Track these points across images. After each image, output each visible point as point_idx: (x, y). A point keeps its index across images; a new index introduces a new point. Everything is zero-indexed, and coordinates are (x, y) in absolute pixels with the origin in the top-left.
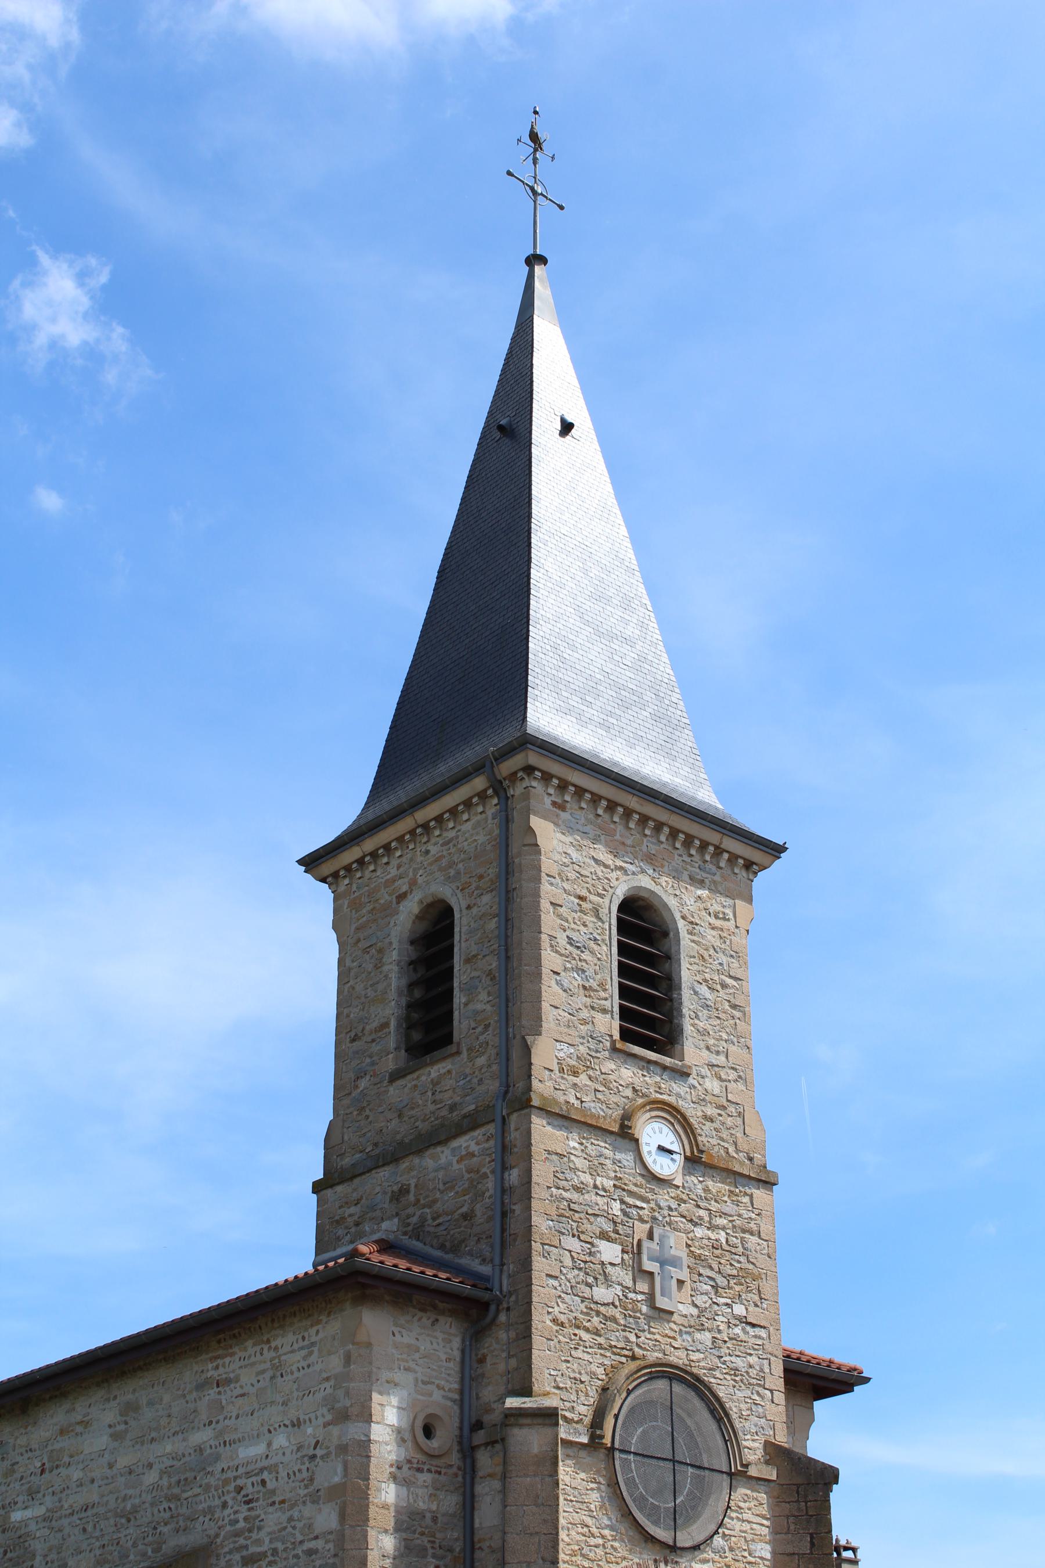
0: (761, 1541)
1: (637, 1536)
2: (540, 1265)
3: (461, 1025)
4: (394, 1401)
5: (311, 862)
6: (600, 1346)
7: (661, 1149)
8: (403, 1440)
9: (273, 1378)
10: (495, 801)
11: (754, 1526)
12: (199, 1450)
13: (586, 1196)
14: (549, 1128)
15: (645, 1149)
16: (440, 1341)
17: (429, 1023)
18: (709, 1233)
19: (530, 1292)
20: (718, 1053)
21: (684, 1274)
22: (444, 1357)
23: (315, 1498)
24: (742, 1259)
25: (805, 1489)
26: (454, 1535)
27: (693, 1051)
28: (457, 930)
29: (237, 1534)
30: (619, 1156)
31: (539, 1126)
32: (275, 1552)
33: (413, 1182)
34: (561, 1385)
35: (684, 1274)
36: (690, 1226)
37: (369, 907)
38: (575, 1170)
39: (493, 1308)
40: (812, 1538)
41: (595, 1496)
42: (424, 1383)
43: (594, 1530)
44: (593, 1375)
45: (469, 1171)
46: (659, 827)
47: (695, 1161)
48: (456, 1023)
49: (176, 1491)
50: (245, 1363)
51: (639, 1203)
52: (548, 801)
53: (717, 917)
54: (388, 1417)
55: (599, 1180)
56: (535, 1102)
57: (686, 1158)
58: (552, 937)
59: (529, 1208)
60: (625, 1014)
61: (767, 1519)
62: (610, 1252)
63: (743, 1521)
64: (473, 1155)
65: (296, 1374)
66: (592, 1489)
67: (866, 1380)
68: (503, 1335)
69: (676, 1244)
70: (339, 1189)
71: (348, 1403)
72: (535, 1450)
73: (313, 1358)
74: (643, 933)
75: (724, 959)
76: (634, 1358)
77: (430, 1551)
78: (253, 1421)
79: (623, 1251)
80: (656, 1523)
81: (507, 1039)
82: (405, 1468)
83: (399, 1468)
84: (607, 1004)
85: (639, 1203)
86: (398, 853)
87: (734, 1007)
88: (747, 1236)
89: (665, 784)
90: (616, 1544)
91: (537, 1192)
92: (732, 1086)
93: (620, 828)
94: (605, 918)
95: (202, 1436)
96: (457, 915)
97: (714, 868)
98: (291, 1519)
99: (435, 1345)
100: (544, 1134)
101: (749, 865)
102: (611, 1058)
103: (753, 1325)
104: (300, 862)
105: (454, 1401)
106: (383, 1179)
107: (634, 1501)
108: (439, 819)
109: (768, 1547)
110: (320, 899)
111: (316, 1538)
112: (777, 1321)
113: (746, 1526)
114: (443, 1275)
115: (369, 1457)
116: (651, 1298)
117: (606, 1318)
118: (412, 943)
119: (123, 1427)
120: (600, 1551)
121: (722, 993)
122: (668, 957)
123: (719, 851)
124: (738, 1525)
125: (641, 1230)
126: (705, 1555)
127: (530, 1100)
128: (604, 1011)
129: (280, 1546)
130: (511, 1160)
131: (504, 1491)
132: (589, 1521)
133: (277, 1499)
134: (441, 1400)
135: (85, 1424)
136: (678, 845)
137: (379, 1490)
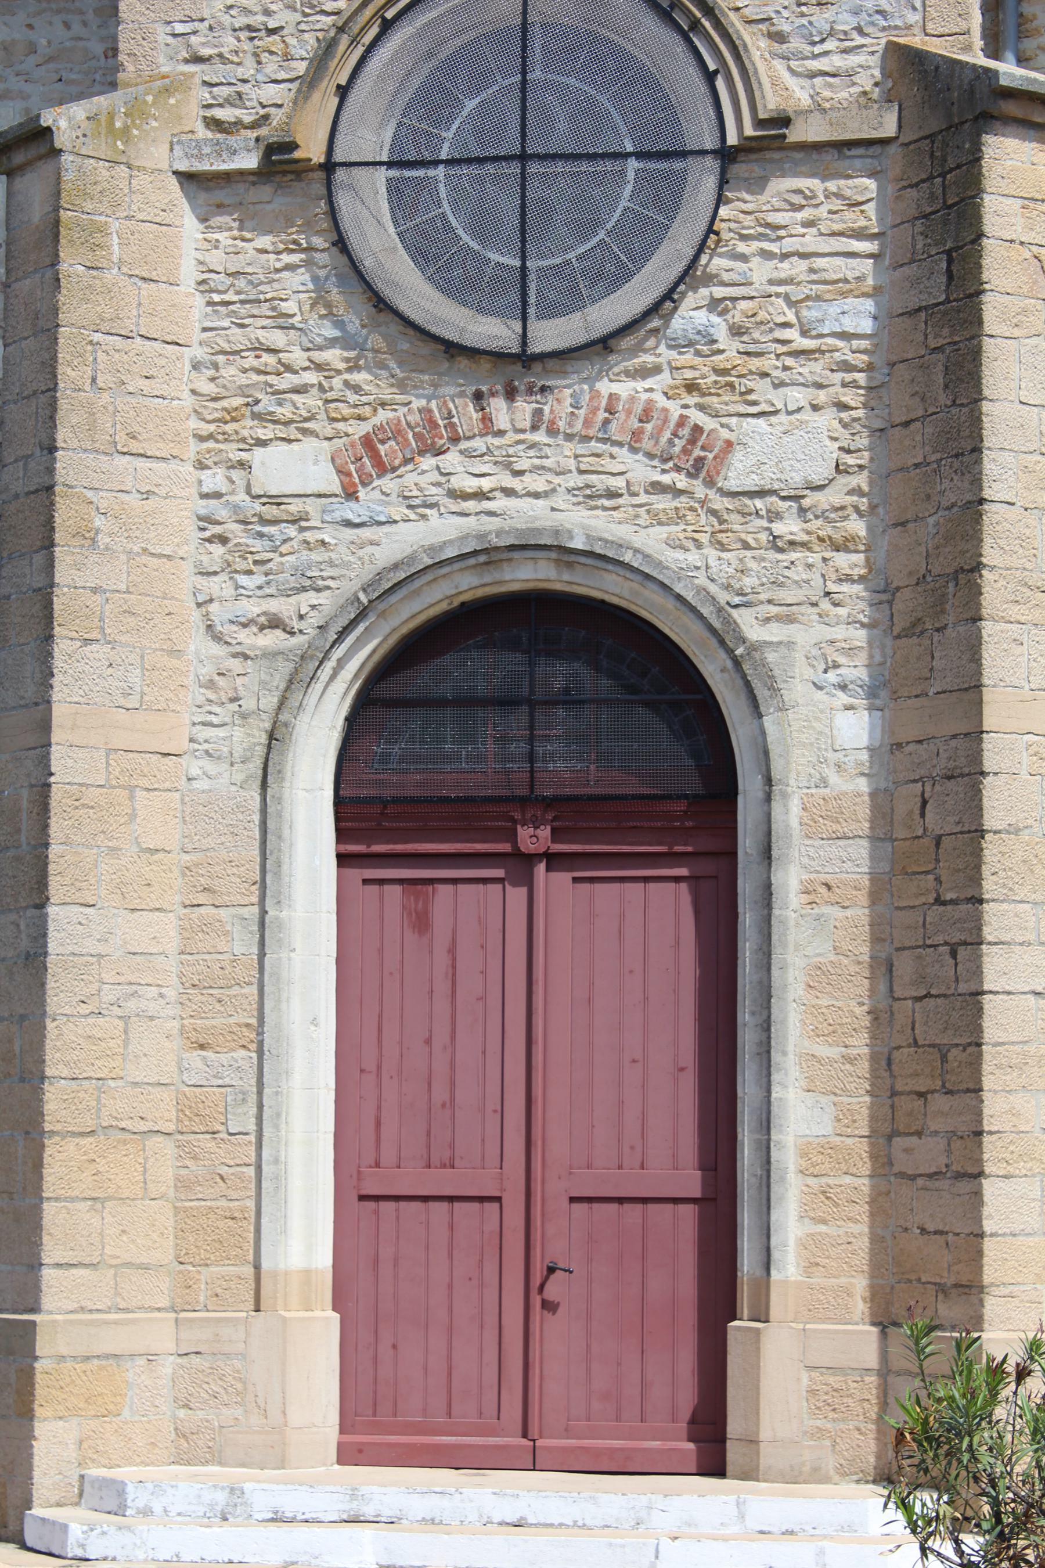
0: (844, 294)
1: (426, 349)
11: (820, 263)
16: (90, 16)
34: (206, 52)
40: (950, 261)
41: (300, 279)
43: (297, 357)
61: (873, 237)
63: (785, 256)
66: (288, 267)
90: (359, 377)
99: (77, 28)
113: (797, 268)
120: (311, 401)
124: (760, 272)
126: (648, 359)
132: (277, 338)
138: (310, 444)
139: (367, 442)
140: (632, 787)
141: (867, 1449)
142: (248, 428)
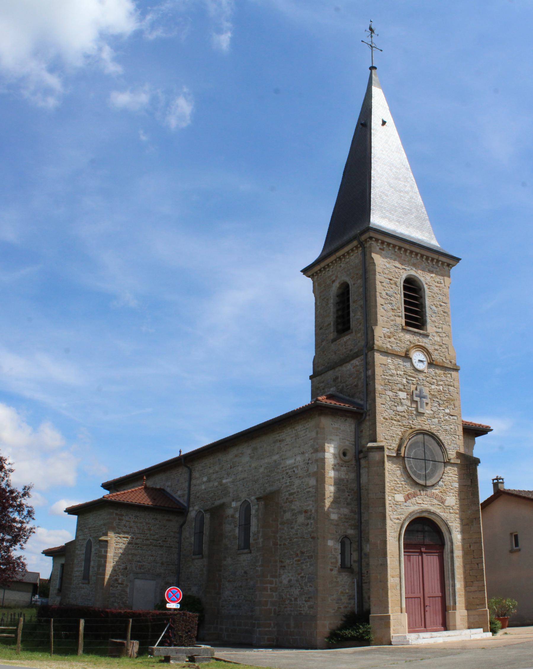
2: (378, 401)
3: (353, 324)
4: (333, 445)
5: (305, 271)
6: (400, 425)
7: (420, 361)
8: (336, 457)
9: (296, 439)
10: (361, 249)
12: (275, 461)
13: (394, 378)
14: (381, 356)
15: (414, 361)
17: (343, 324)
18: (437, 387)
19: (375, 409)
20: (439, 328)
21: (428, 401)
22: (349, 431)
23: (309, 476)
24: (448, 395)
25: (469, 466)
26: (354, 486)
27: (430, 328)
28: (350, 292)
29: (287, 487)
30: (405, 364)
31: (377, 355)
32: (298, 492)
33: (339, 375)
35: (428, 401)
36: (430, 385)
37: (323, 285)
38: (390, 369)
39: (364, 415)
41: (399, 472)
42: (343, 439)
43: (399, 482)
44: (398, 434)
45: (356, 371)
46: (417, 254)
47: (431, 364)
48: (351, 323)
49: (269, 474)
50: (287, 435)
51: (412, 379)
52: (378, 248)
53: (438, 283)
54: (330, 451)
55: (398, 372)
56: (376, 348)
57: (428, 363)
58: (380, 293)
59: (374, 383)
60: (407, 317)
62: (402, 395)
64: (357, 366)
65: (302, 438)
67: (492, 430)
68: (368, 423)
69: (426, 391)
70: (317, 378)
71: (318, 446)
72: (377, 459)
73: (307, 433)
74: (413, 290)
75: (441, 297)
76: (411, 428)
77: (346, 491)
78: (289, 452)
79: (407, 395)
80: (419, 479)
81: (367, 328)
82: (337, 466)
83: (335, 466)
84: (400, 314)
85: (412, 379)
86: (332, 267)
87: (444, 312)
88: (450, 387)
89: (419, 240)
90: (406, 486)
91: (377, 377)
92: (444, 339)
93: (403, 255)
94: (399, 286)
95: (276, 457)
96: (350, 287)
97: (437, 267)
98: (302, 482)
100: (378, 358)
101: (448, 265)
102: (402, 332)
103: (452, 416)
104: (302, 271)
105: (353, 444)
106: (330, 375)
107: (412, 473)
108: (344, 255)
109: (458, 484)
110: (308, 283)
111: (310, 487)
112: (460, 414)
114: (347, 405)
115: (325, 463)
116: (417, 409)
117: (402, 416)
118: (337, 296)
119: (253, 455)
120: (401, 489)
121: (440, 308)
122: (421, 297)
123: (438, 261)
125: (413, 387)
127: (374, 347)
128: (399, 316)
129: (299, 490)
130: (369, 367)
131: (368, 472)
132: (397, 480)
133: (298, 476)
134: (348, 443)
135: (242, 454)
136: (424, 260)
137: (328, 473)
138: (401, 495)
139: (408, 495)
140: (432, 543)
141: (466, 625)
142: (394, 491)
